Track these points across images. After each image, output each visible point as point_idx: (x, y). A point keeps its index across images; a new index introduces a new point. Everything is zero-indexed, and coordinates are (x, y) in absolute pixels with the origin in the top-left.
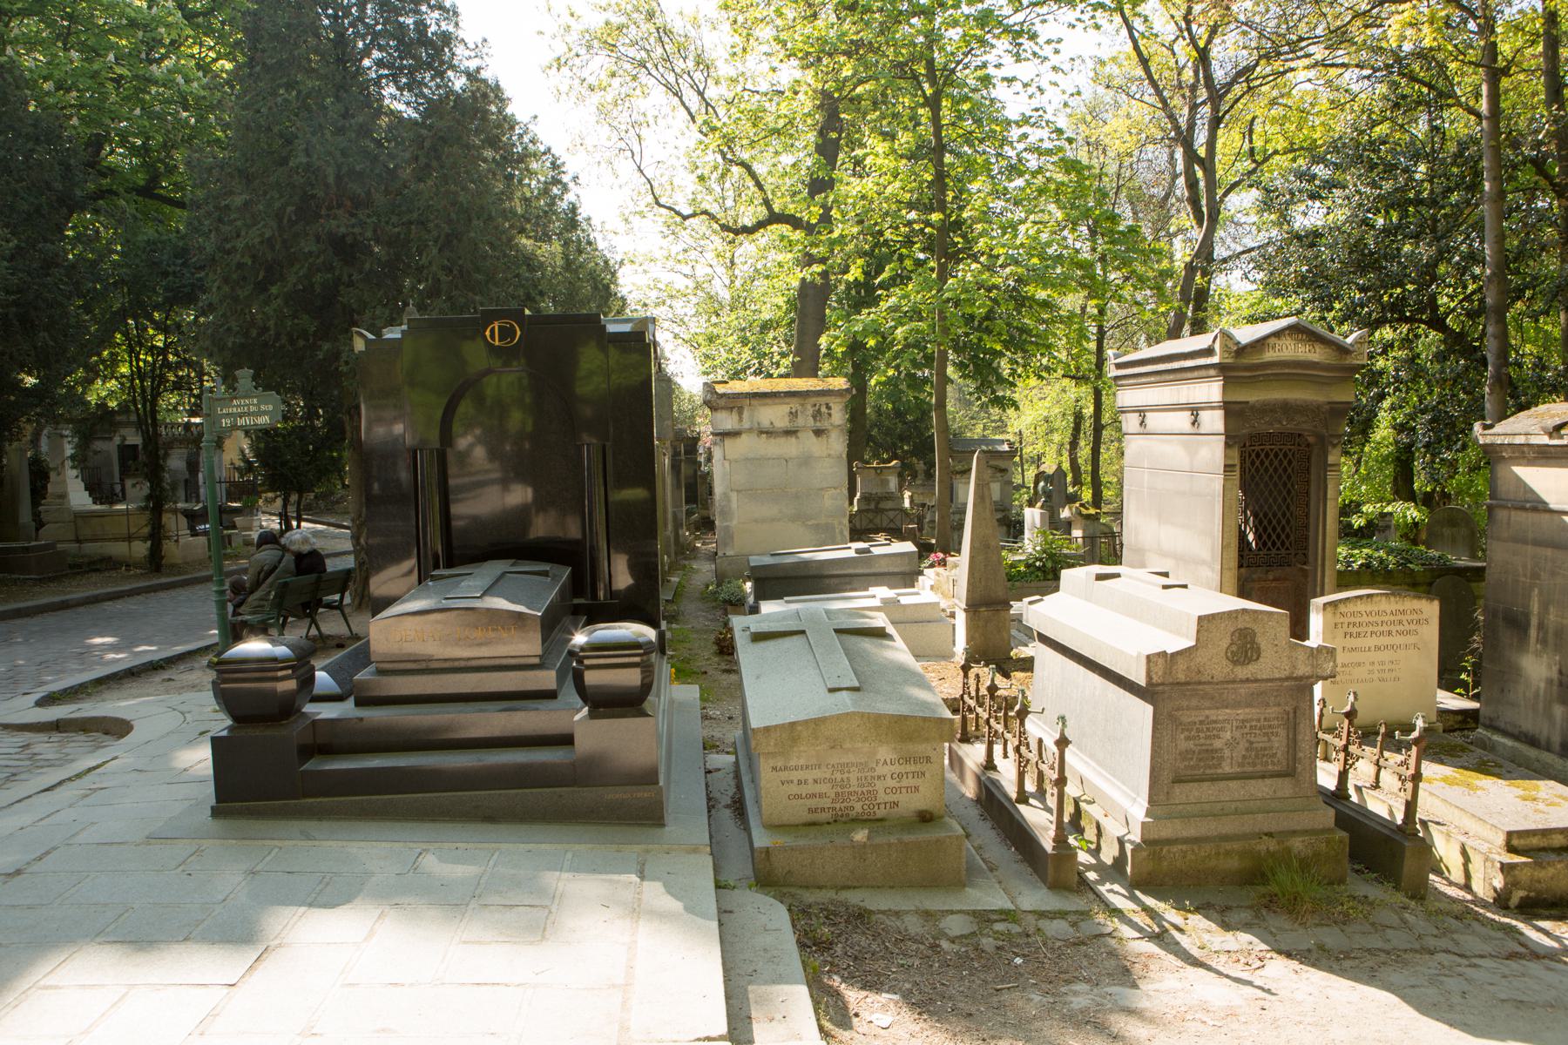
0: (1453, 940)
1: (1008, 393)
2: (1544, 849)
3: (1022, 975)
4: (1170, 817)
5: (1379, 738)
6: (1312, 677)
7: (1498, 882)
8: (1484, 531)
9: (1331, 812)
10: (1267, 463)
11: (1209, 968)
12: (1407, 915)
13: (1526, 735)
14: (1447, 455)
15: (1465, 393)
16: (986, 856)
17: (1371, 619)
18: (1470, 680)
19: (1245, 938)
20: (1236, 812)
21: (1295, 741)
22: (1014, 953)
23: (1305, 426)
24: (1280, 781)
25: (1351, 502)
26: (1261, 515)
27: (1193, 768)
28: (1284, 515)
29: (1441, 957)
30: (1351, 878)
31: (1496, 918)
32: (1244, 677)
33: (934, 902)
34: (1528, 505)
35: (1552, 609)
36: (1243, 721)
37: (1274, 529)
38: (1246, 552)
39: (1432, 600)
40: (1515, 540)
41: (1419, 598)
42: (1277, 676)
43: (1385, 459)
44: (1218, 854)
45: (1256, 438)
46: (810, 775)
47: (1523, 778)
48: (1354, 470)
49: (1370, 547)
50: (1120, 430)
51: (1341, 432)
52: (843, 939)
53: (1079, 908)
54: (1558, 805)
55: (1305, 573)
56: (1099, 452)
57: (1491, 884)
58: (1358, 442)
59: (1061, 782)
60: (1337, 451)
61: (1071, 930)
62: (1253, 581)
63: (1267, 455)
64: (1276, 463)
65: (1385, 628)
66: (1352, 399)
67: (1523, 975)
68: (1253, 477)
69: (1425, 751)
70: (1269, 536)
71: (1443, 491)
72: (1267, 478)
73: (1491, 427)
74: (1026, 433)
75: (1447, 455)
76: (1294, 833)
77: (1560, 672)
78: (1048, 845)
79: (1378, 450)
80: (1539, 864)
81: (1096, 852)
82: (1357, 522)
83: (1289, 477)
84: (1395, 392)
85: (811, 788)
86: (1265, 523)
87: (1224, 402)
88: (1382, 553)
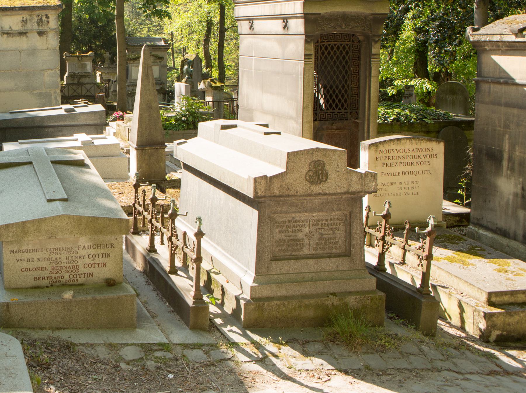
0: (453, 363)
1: (164, 8)
2: (512, 304)
3: (173, 385)
4: (269, 283)
5: (405, 232)
6: (361, 192)
7: (483, 325)
8: (473, 97)
9: (374, 280)
10: (332, 53)
11: (294, 381)
12: (423, 347)
13: (500, 230)
14: (449, 48)
15: (461, 8)
16: (149, 308)
17: (399, 154)
18: (464, 194)
19: (318, 361)
20: (312, 280)
21: (350, 233)
22: (168, 371)
23: (357, 29)
24: (340, 259)
25: (387, 78)
26: (328, 87)
27: (284, 251)
28: (343, 87)
29: (445, 374)
30: (387, 322)
31: (481, 348)
32: (317, 192)
33: (116, 338)
34: (502, 81)
35: (517, 148)
36: (317, 221)
37: (337, 96)
38: (319, 111)
39: (439, 142)
40: (494, 103)
41: (431, 141)
42: (339, 191)
43: (409, 50)
44: (300, 307)
45: (325, 37)
46: (35, 256)
47: (498, 257)
48: (389, 57)
49: (399, 107)
50: (237, 32)
51: (380, 33)
52: (56, 362)
53: (210, 342)
54: (521, 275)
55: (357, 125)
56: (223, 46)
57: (478, 326)
58: (391, 39)
59: (199, 260)
60: (378, 45)
61: (205, 356)
62: (323, 130)
63: (332, 48)
64: (338, 53)
65: (409, 160)
66: (387, 11)
67: (499, 385)
68: (323, 63)
69: (435, 240)
70: (334, 101)
71: (446, 71)
72: (332, 63)
73: (478, 30)
74: (176, 34)
75: (449, 48)
76: (350, 293)
77: (523, 189)
78: (190, 301)
79: (404, 45)
80: (509, 314)
81: (221, 306)
82: (391, 91)
83: (347, 62)
84: (415, 7)
85: (36, 264)
86: (331, 92)
87: (304, 14)
88: (407, 112)
